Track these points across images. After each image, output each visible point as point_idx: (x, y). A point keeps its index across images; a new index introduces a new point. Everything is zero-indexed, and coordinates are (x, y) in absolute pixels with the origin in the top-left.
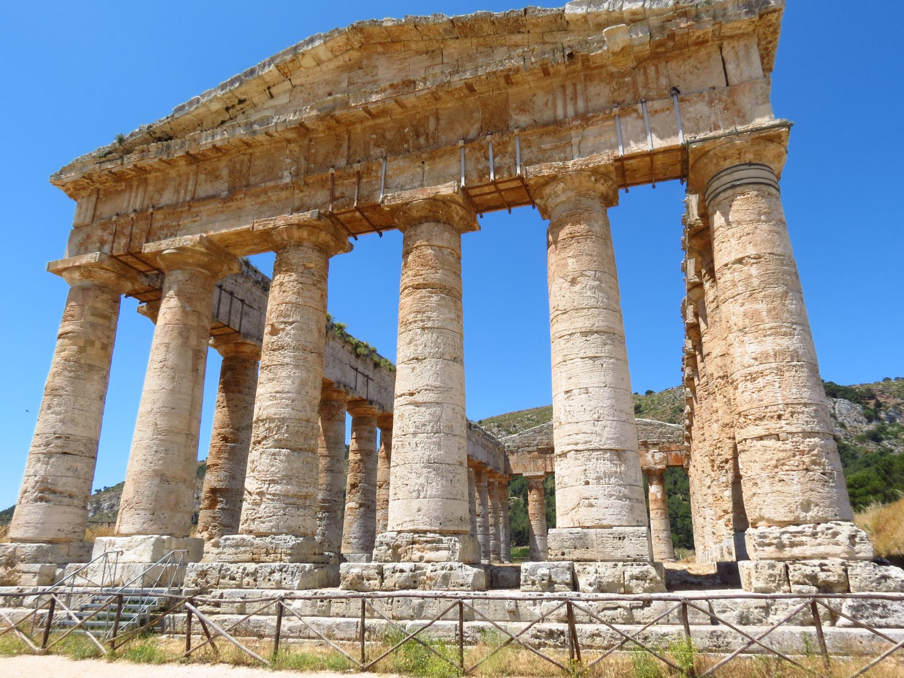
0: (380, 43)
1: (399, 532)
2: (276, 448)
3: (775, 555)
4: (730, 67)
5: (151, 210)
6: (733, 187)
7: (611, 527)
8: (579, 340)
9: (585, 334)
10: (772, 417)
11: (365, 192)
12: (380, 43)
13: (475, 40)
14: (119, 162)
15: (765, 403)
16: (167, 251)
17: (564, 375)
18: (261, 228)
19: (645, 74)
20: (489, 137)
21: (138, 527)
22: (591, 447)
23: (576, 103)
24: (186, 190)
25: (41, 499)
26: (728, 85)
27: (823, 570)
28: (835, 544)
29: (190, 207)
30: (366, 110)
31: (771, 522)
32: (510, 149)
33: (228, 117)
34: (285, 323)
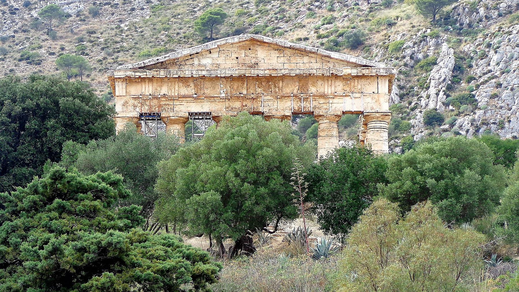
14: (145, 73)
20: (302, 95)
30: (258, 75)
32: (309, 100)
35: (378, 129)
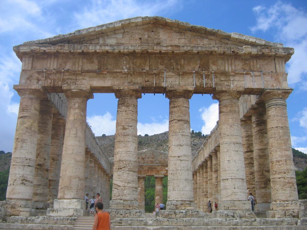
0: (161, 24)
1: (177, 201)
2: (129, 171)
3: (282, 209)
4: (277, 66)
5: (63, 71)
6: (276, 105)
7: (241, 201)
8: (233, 146)
9: (234, 144)
10: (283, 173)
11: (157, 82)
12: (161, 24)
13: (197, 34)
14: (50, 48)
15: (281, 169)
16: (74, 90)
17: (227, 155)
18: (117, 88)
19: (253, 62)
20: (204, 72)
21: (72, 196)
22: (236, 178)
23: (232, 66)
24: (78, 65)
25: (23, 183)
26: (276, 72)
27: (293, 213)
28: (296, 206)
29: (82, 72)
30: (160, 52)
31: (280, 201)
32: (210, 77)
33: (96, 37)
34: (128, 126)
35: (280, 106)
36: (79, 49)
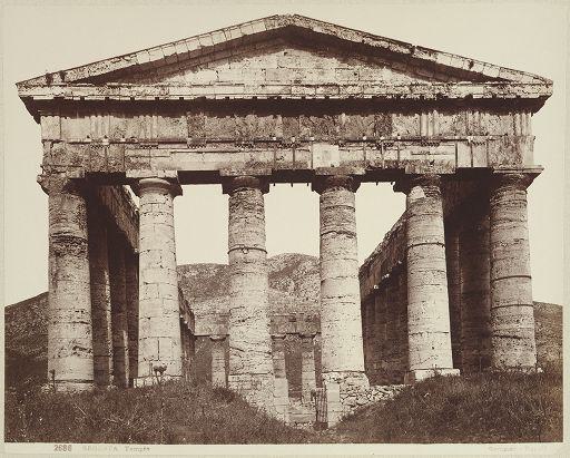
5: (123, 140)
36: (148, 91)
